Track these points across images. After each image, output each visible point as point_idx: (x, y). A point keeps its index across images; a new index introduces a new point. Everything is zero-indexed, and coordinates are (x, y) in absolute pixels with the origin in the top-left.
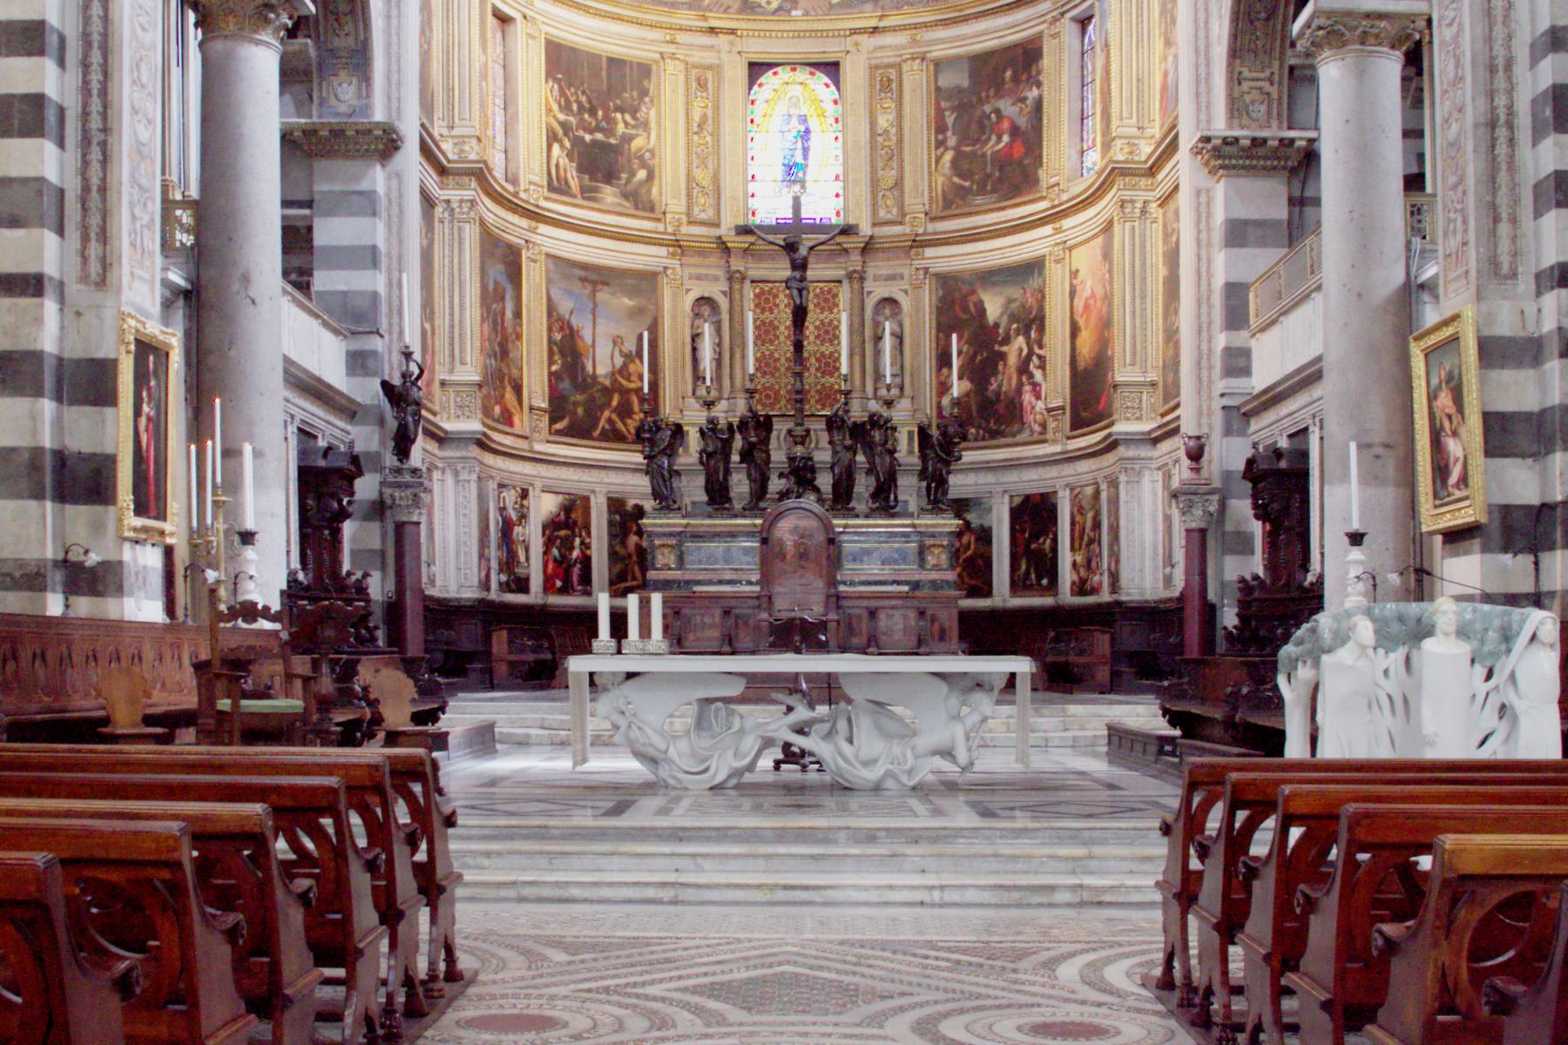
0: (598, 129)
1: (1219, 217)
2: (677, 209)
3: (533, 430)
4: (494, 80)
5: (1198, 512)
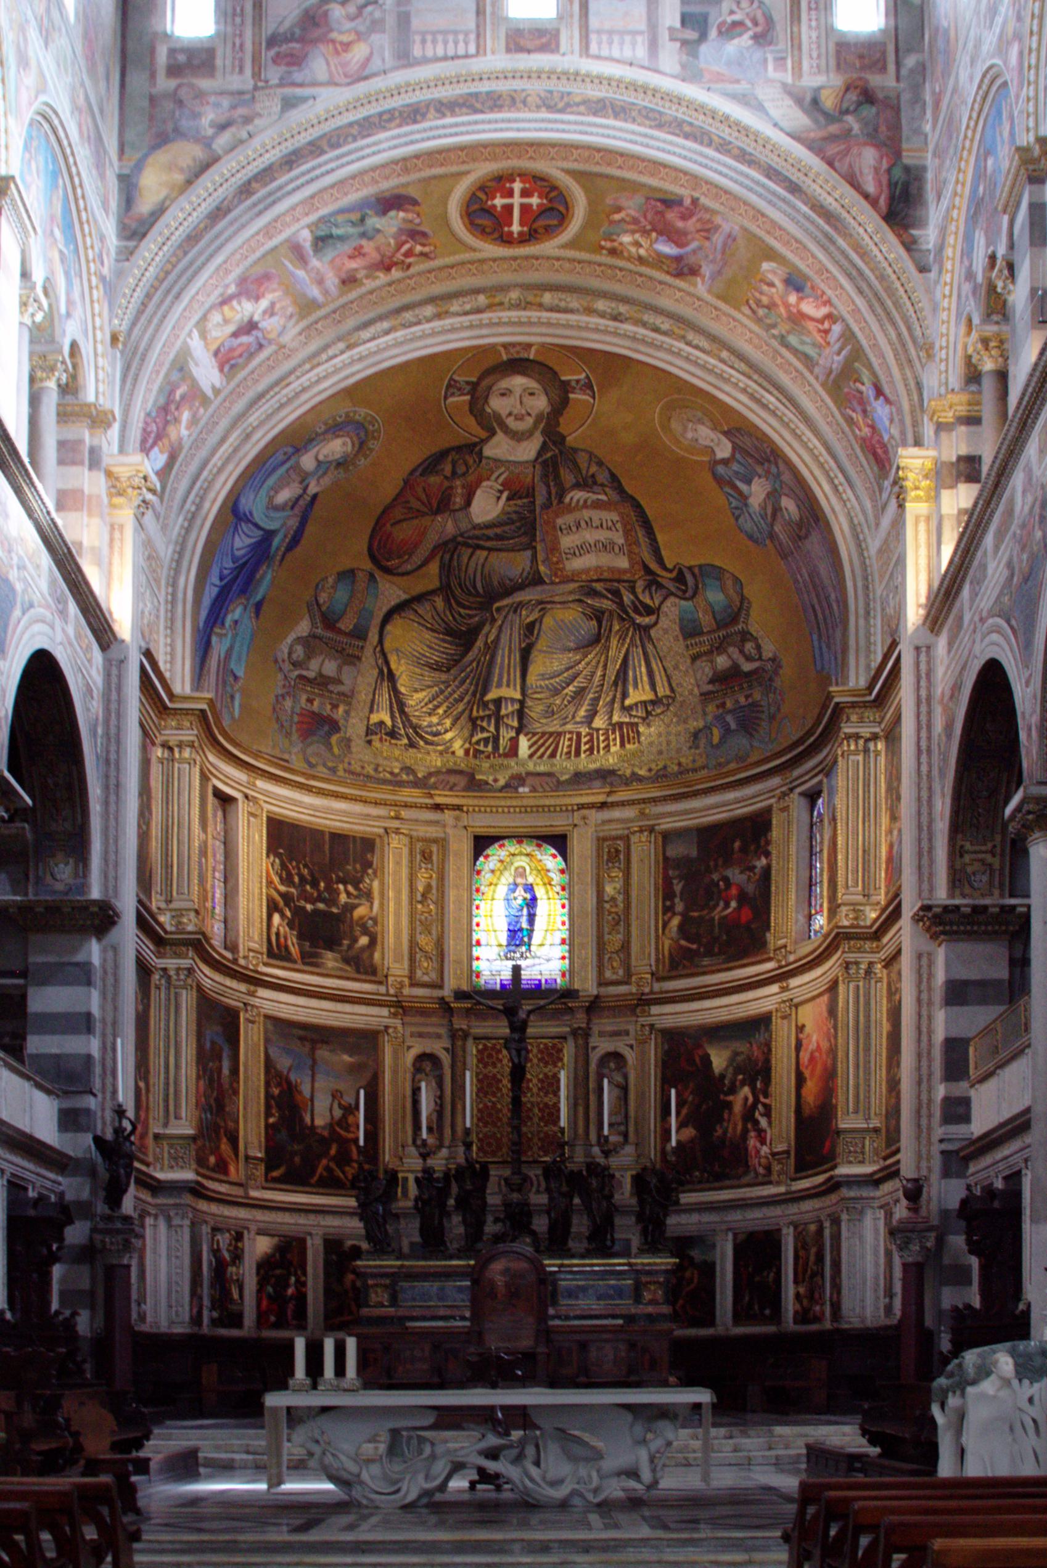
0: (320, 899)
2: (399, 973)
4: (214, 856)
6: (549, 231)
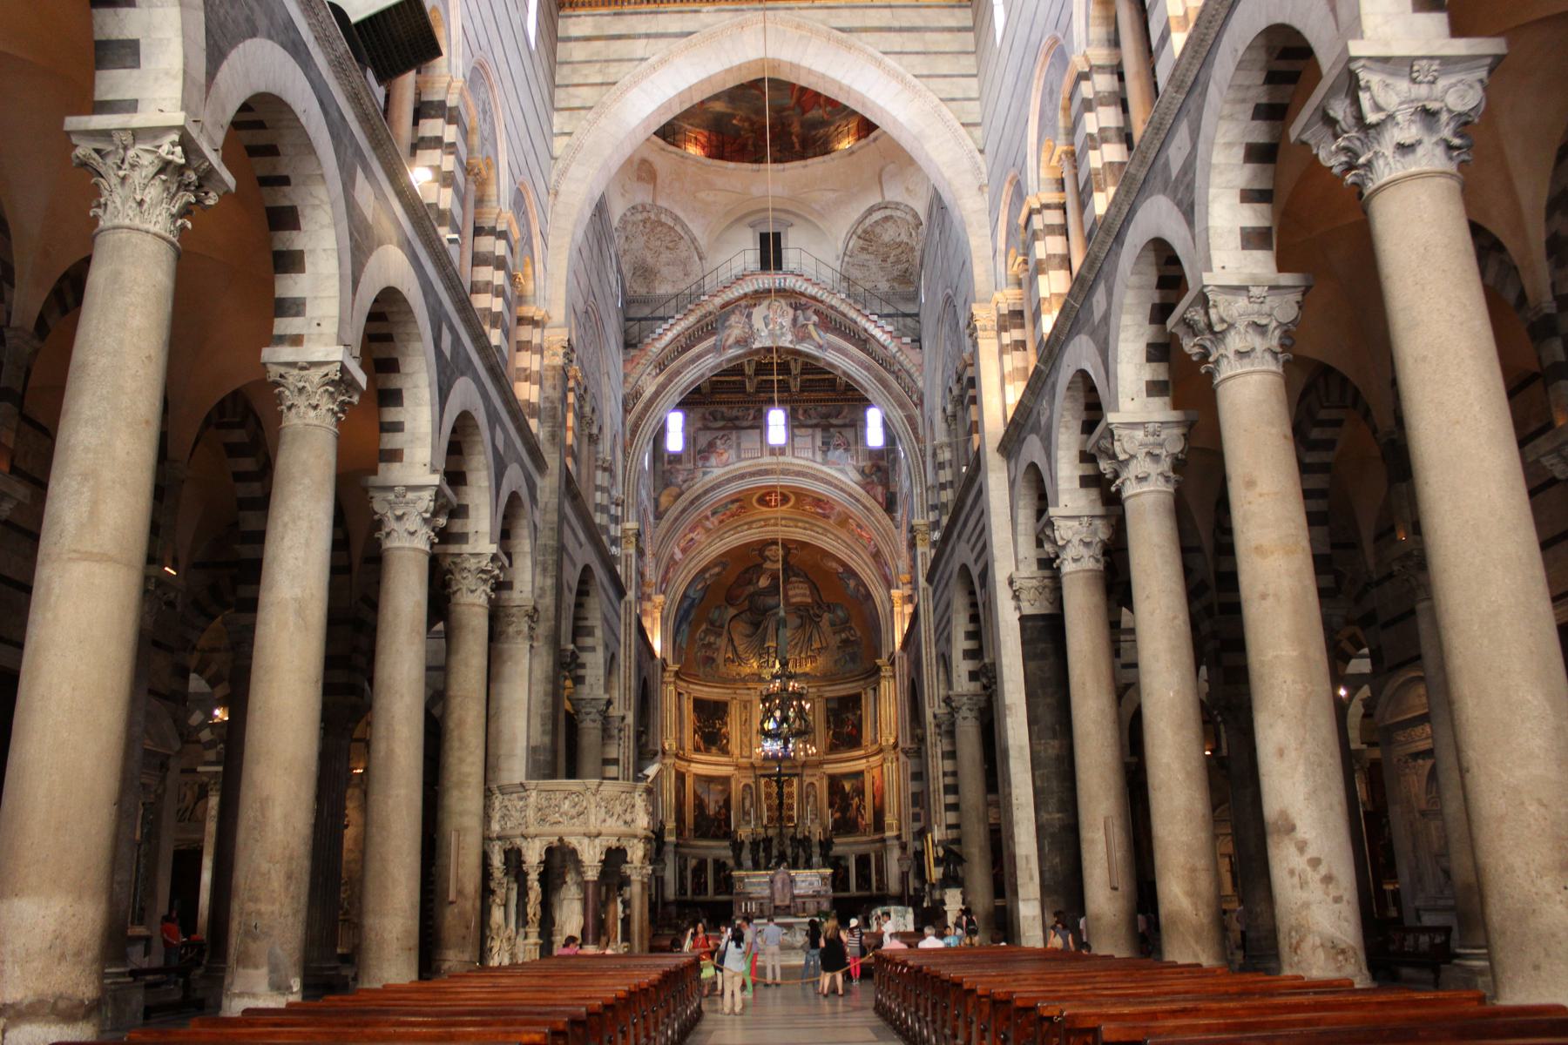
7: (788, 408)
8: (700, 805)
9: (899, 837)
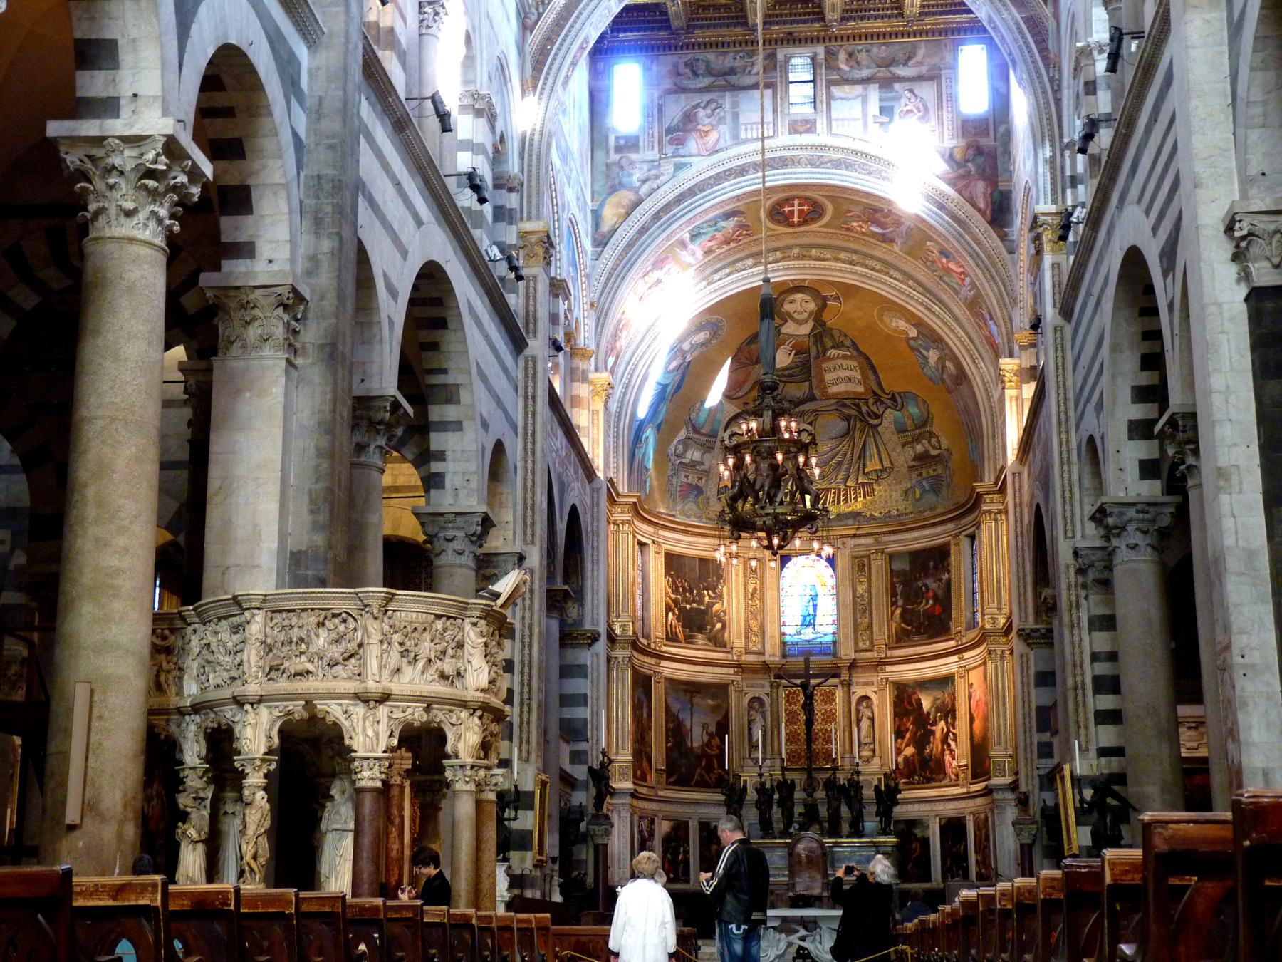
1: (1032, 671)
3: (659, 782)
5: (1025, 834)
6: (813, 220)
7: (820, 51)
8: (676, 731)
9: (1014, 786)
